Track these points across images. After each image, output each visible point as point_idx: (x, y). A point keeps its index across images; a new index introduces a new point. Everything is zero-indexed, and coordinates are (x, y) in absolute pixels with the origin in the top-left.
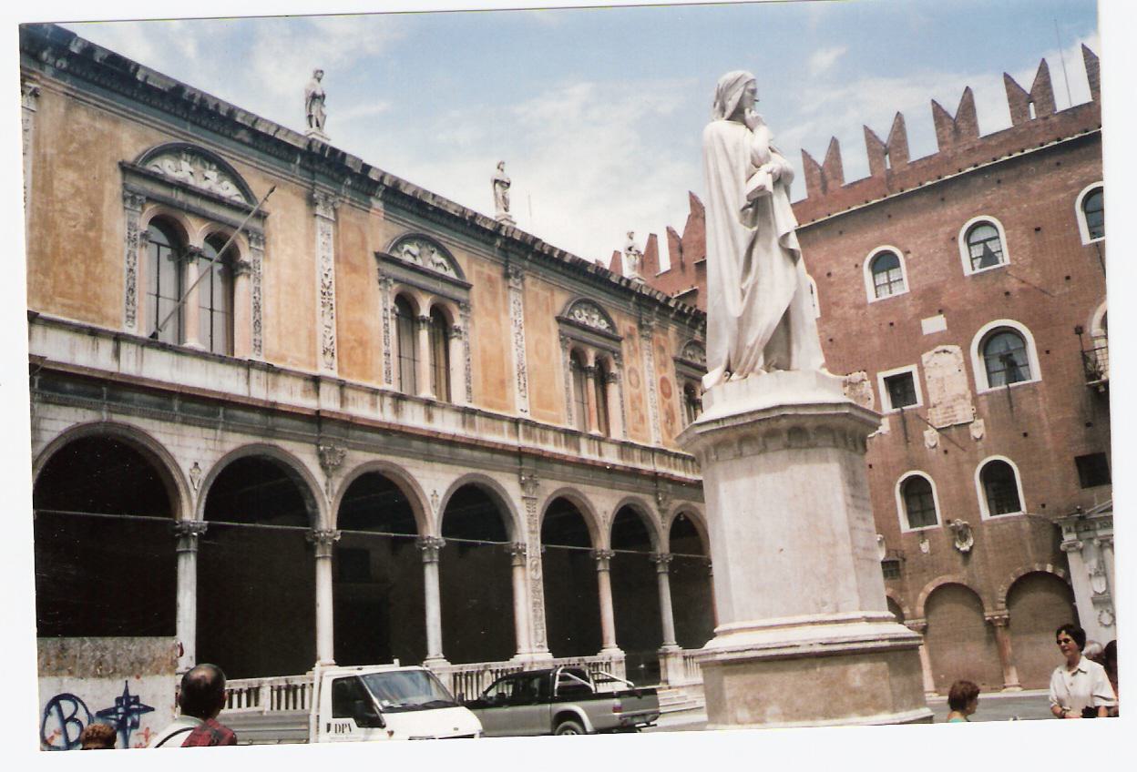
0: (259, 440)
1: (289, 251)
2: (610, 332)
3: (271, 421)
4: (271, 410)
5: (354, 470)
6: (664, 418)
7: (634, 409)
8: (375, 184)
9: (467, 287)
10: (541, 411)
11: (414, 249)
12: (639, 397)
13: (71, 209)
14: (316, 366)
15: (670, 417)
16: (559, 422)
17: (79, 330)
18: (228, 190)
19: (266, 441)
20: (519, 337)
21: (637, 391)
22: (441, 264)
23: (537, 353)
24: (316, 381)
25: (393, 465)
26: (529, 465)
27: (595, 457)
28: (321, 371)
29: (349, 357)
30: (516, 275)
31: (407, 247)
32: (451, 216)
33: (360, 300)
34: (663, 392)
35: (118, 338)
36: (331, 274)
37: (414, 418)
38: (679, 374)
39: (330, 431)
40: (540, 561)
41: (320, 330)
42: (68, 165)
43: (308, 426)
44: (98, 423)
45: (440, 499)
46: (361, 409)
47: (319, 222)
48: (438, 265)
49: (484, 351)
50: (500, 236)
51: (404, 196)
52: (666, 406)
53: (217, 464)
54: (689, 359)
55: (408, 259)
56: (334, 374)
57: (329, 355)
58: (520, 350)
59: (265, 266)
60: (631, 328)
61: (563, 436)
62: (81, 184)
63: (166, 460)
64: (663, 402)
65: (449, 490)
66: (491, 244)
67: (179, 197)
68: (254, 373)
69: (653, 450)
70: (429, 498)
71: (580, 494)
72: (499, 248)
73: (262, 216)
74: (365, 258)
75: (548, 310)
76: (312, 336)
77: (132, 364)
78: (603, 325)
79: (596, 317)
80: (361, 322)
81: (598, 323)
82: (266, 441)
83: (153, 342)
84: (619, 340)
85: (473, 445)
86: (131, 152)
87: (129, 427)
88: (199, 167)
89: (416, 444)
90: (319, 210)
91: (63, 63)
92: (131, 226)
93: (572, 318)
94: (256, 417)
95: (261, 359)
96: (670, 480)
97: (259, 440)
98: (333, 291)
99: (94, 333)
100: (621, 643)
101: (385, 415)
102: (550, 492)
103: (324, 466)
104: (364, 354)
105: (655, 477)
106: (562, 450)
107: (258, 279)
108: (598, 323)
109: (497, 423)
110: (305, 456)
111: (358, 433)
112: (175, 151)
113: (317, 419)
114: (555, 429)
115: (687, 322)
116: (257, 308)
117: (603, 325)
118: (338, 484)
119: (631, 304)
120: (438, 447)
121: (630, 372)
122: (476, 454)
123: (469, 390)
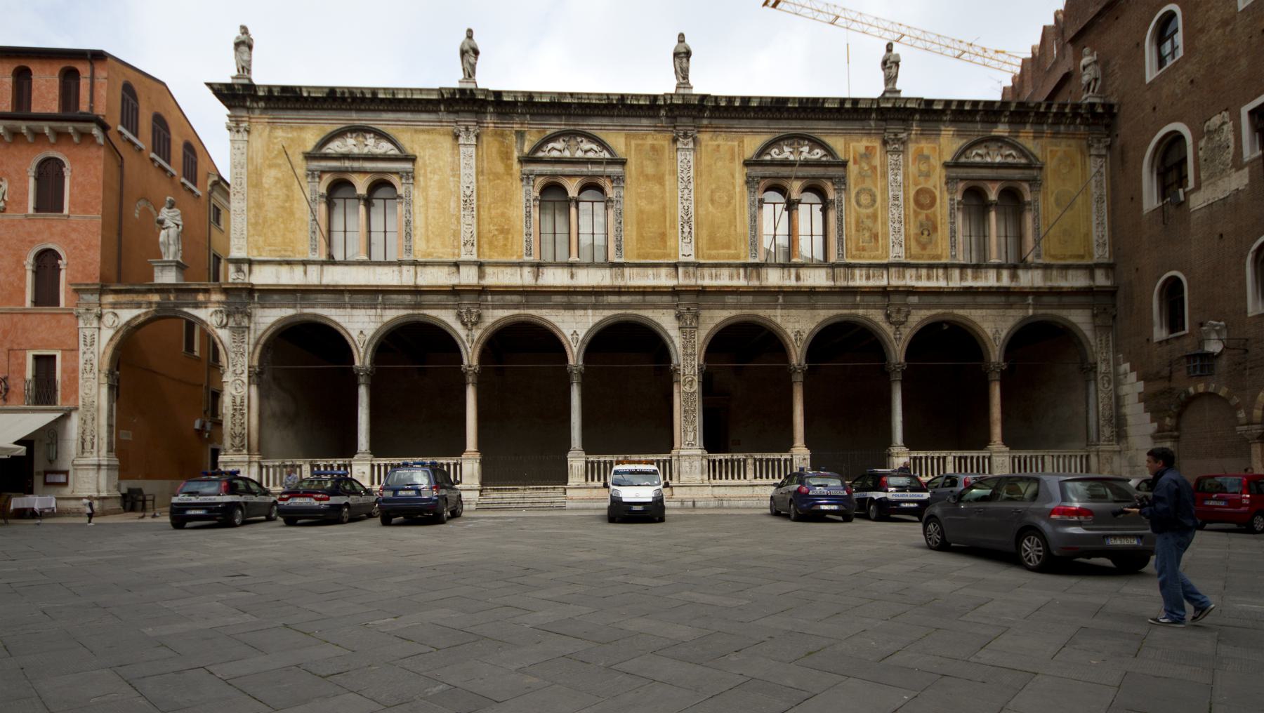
0: (410, 312)
1: (436, 177)
2: (829, 158)
3: (419, 298)
4: (416, 291)
5: (493, 324)
6: (913, 230)
7: (859, 226)
8: (514, 104)
9: (623, 163)
10: (713, 252)
11: (559, 145)
12: (874, 217)
13: (274, 193)
14: (459, 255)
15: (929, 228)
16: (738, 258)
17: (280, 263)
18: (385, 148)
19: (416, 312)
20: (686, 191)
21: (870, 211)
22: (591, 150)
23: (712, 201)
24: (456, 265)
25: (532, 316)
26: (686, 300)
27: (792, 282)
28: (464, 257)
29: (491, 243)
30: (685, 136)
31: (550, 145)
32: (596, 106)
33: (506, 199)
34: (917, 202)
35: (305, 263)
36: (474, 186)
37: (554, 278)
38: (950, 181)
39: (466, 300)
40: (696, 378)
41: (463, 228)
42: (270, 166)
43: (451, 298)
44: (295, 316)
45: (581, 337)
46: (496, 278)
47: (462, 149)
48: (586, 152)
49: (641, 212)
50: (660, 107)
51: (544, 104)
52: (922, 217)
53: (378, 331)
54: (978, 159)
55: (555, 154)
56: (474, 258)
57: (469, 246)
58: (686, 204)
59: (417, 195)
60: (867, 148)
61: (742, 271)
62: (280, 175)
63: (342, 332)
64: (916, 214)
65: (590, 331)
66: (657, 116)
67: (347, 164)
68: (405, 268)
69: (887, 266)
70: (569, 338)
71: (763, 318)
72: (667, 116)
73: (412, 159)
74: (509, 168)
75: (732, 159)
76: (456, 234)
77: (313, 277)
78: (818, 154)
79: (806, 149)
80: (503, 215)
81: (805, 153)
82: (416, 312)
83: (331, 261)
84: (844, 164)
85: (619, 291)
86: (310, 146)
87: (315, 315)
88: (361, 139)
89: (558, 299)
90: (461, 141)
91: (262, 104)
92: (314, 191)
93: (768, 158)
94: (408, 298)
95: (412, 258)
96: (911, 291)
97: (410, 312)
98: (474, 197)
99: (289, 263)
100: (808, 444)
101: (524, 278)
102: (717, 321)
103: (464, 324)
104: (506, 239)
105: (884, 292)
106: (742, 282)
107: (409, 203)
108: (805, 153)
109: (650, 271)
110: (447, 317)
111: (496, 297)
112: (340, 134)
113: (455, 292)
114: (729, 266)
115: (978, 118)
116: (408, 223)
117: (818, 154)
118: (477, 333)
119: (872, 123)
120: (580, 298)
121: (858, 194)
122: (625, 299)
123: (619, 248)
